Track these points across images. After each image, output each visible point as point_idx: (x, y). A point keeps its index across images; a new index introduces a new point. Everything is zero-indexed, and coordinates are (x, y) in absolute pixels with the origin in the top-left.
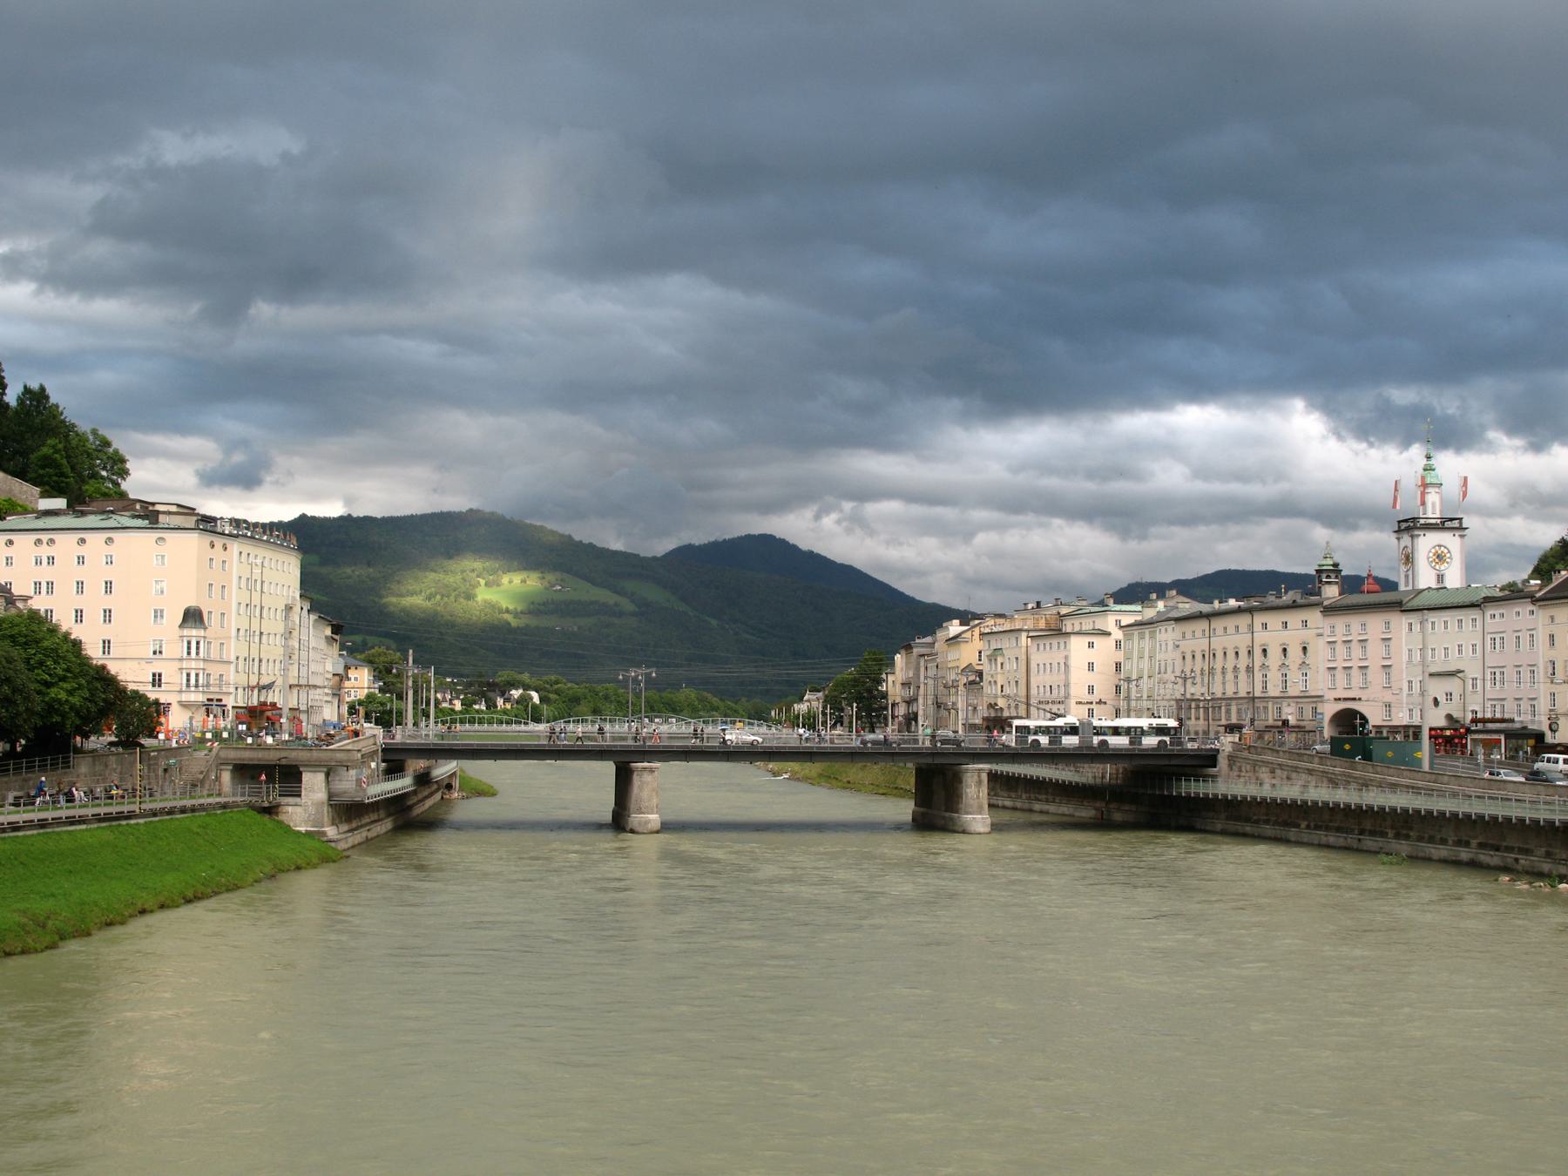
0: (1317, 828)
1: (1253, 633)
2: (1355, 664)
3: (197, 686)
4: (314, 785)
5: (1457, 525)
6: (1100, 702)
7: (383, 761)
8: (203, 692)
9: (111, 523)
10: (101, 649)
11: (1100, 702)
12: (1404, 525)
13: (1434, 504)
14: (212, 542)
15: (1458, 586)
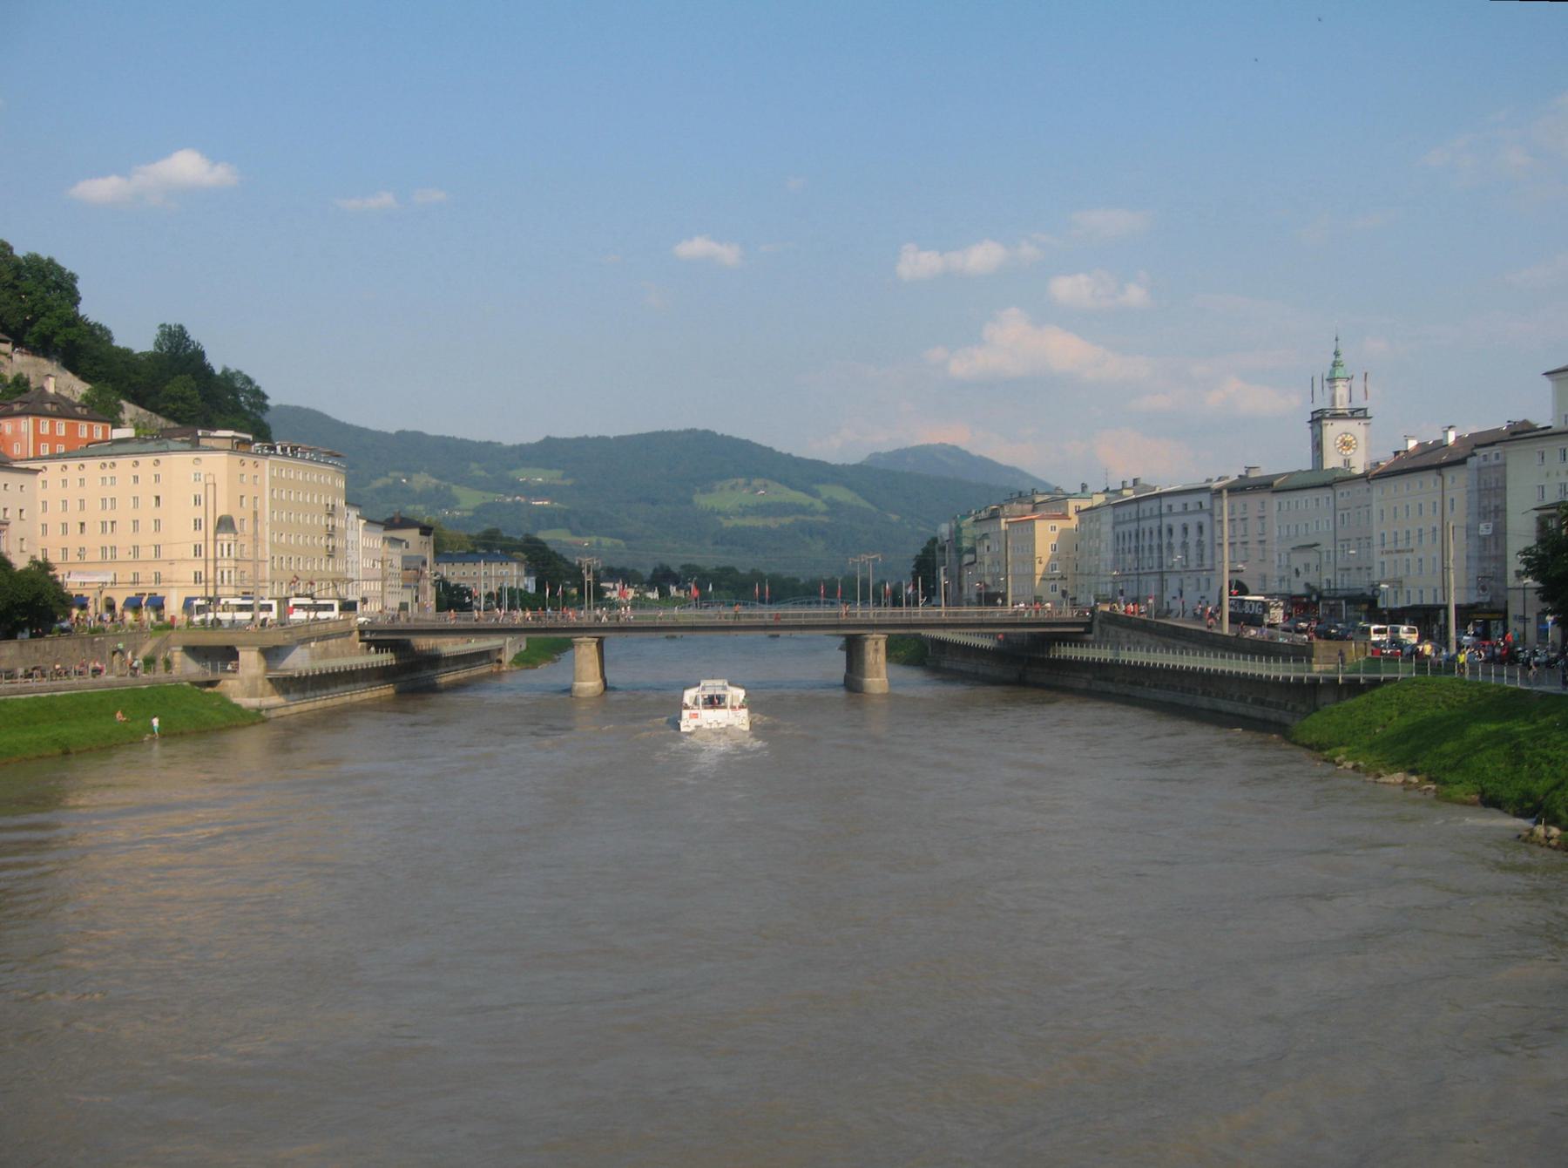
0: (1156, 686)
2: (1239, 539)
3: (229, 581)
4: (250, 661)
5: (1362, 415)
6: (1062, 578)
7: (361, 641)
8: (236, 587)
9: (164, 447)
10: (61, 555)
11: (1062, 578)
12: (1316, 416)
14: (242, 460)
15: (1310, 468)
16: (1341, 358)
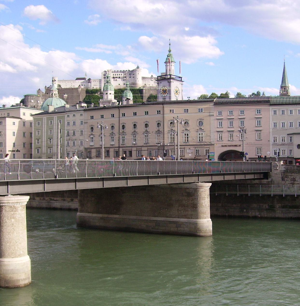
1: (119, 118)
13: (173, 70)
16: (171, 53)
